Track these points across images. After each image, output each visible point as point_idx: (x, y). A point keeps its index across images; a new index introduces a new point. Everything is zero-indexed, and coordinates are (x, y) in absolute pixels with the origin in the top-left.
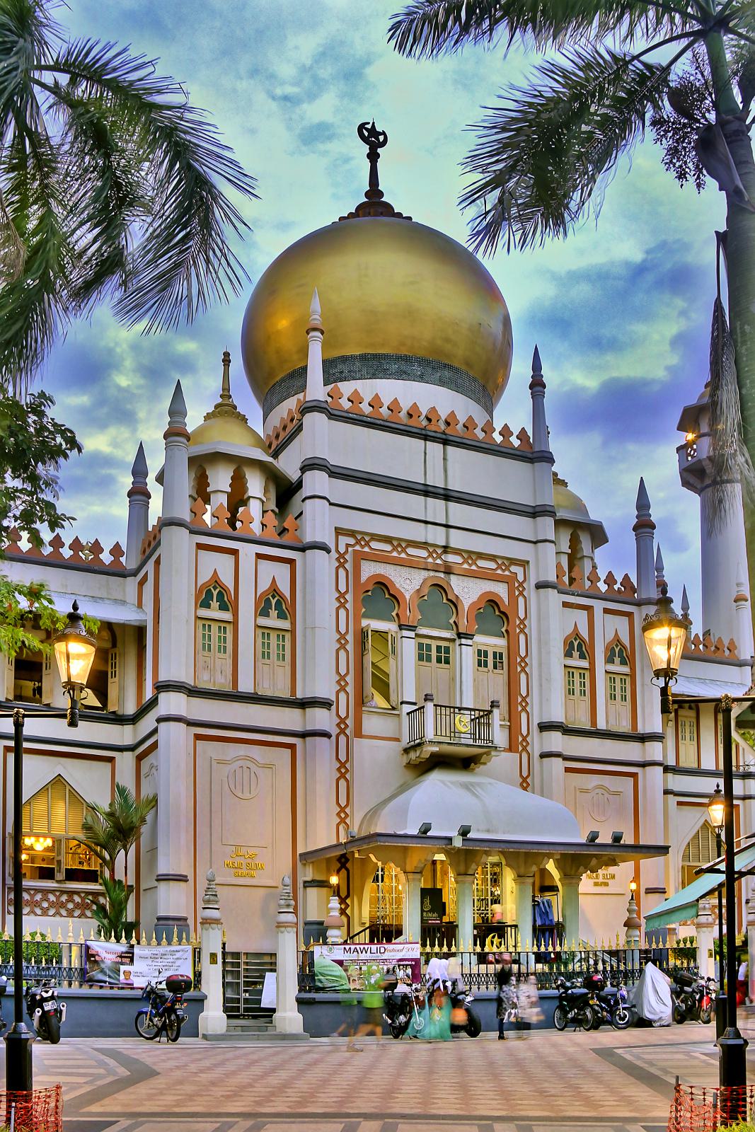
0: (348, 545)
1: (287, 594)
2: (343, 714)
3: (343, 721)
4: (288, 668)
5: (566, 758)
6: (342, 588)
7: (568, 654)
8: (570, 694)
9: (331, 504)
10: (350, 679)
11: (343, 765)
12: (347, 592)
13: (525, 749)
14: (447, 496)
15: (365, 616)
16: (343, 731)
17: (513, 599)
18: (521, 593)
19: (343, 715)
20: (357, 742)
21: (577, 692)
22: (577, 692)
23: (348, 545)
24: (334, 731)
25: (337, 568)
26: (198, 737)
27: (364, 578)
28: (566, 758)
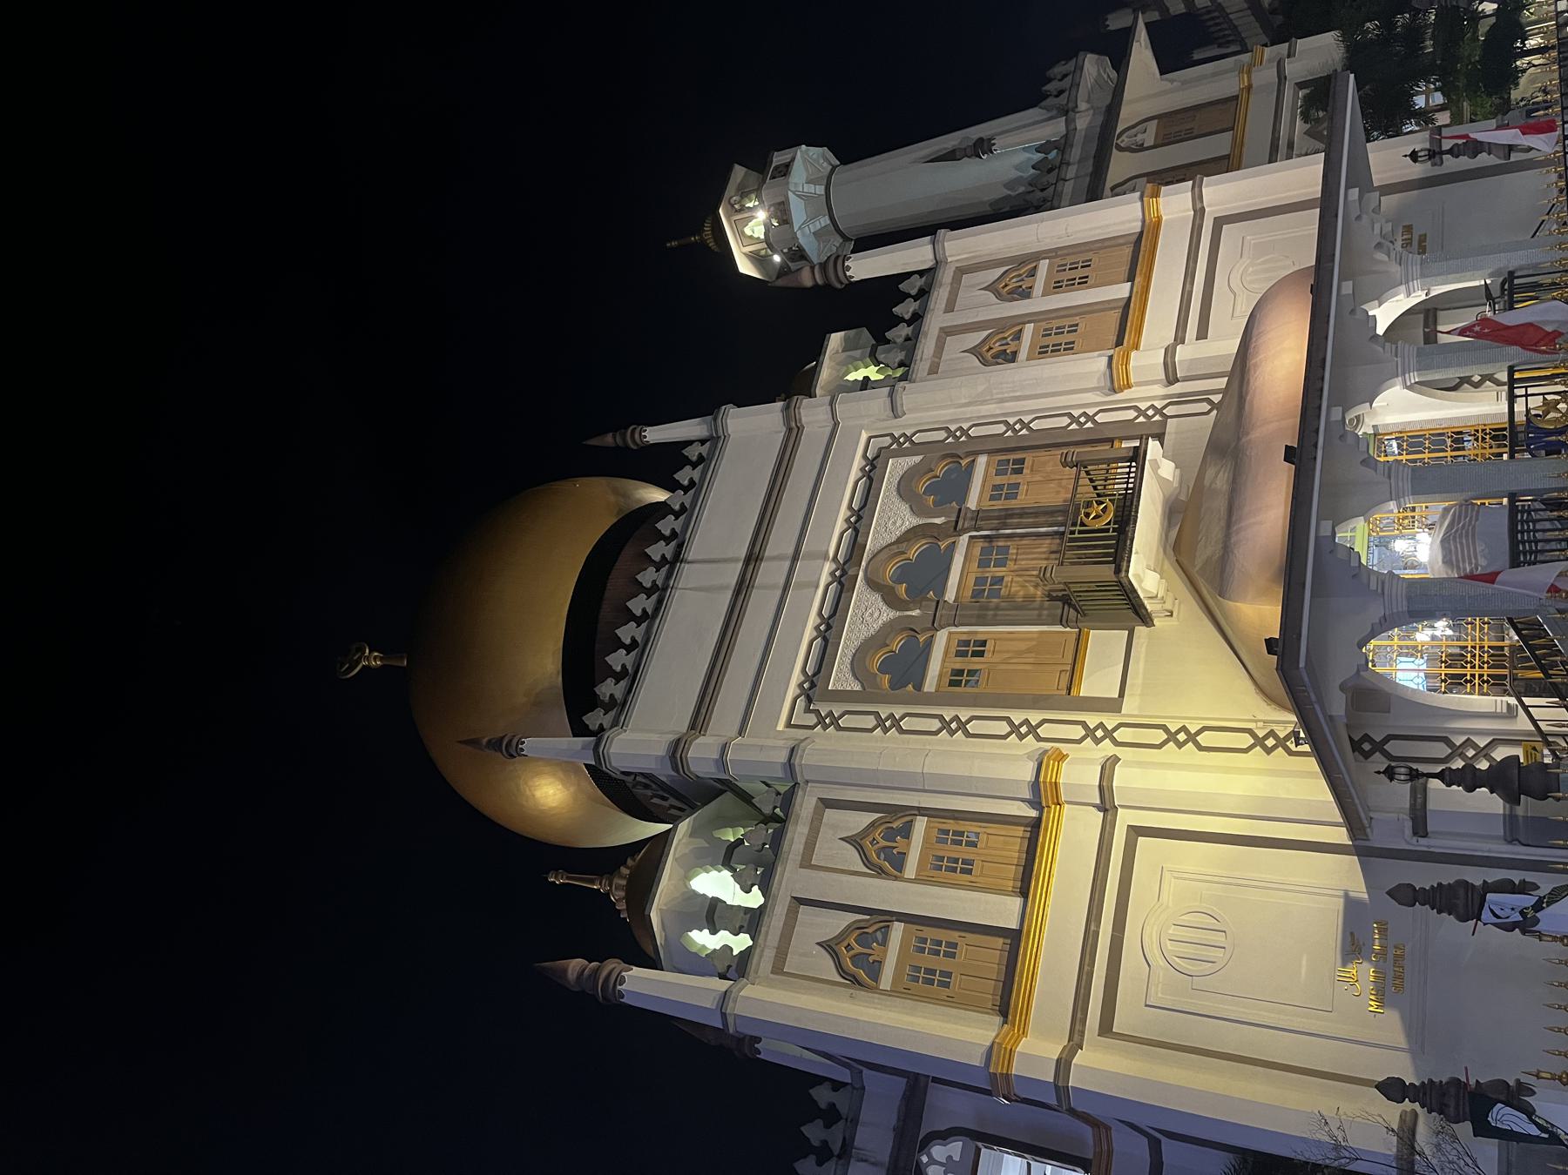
0: (807, 710)
1: (867, 818)
2: (1078, 732)
3: (1090, 732)
4: (993, 828)
5: (1180, 338)
6: (870, 722)
7: (1012, 358)
8: (1072, 348)
9: (741, 732)
10: (1017, 716)
11: (1172, 737)
12: (877, 714)
13: (1159, 411)
14: (753, 558)
15: (919, 686)
16: (1109, 734)
17: (916, 448)
18: (908, 439)
19: (1078, 732)
20: (1128, 706)
21: (1070, 338)
22: (1070, 338)
23: (807, 710)
24: (1107, 748)
25: (839, 728)
26: (1106, 1028)
27: (857, 687)
28: (1180, 338)
